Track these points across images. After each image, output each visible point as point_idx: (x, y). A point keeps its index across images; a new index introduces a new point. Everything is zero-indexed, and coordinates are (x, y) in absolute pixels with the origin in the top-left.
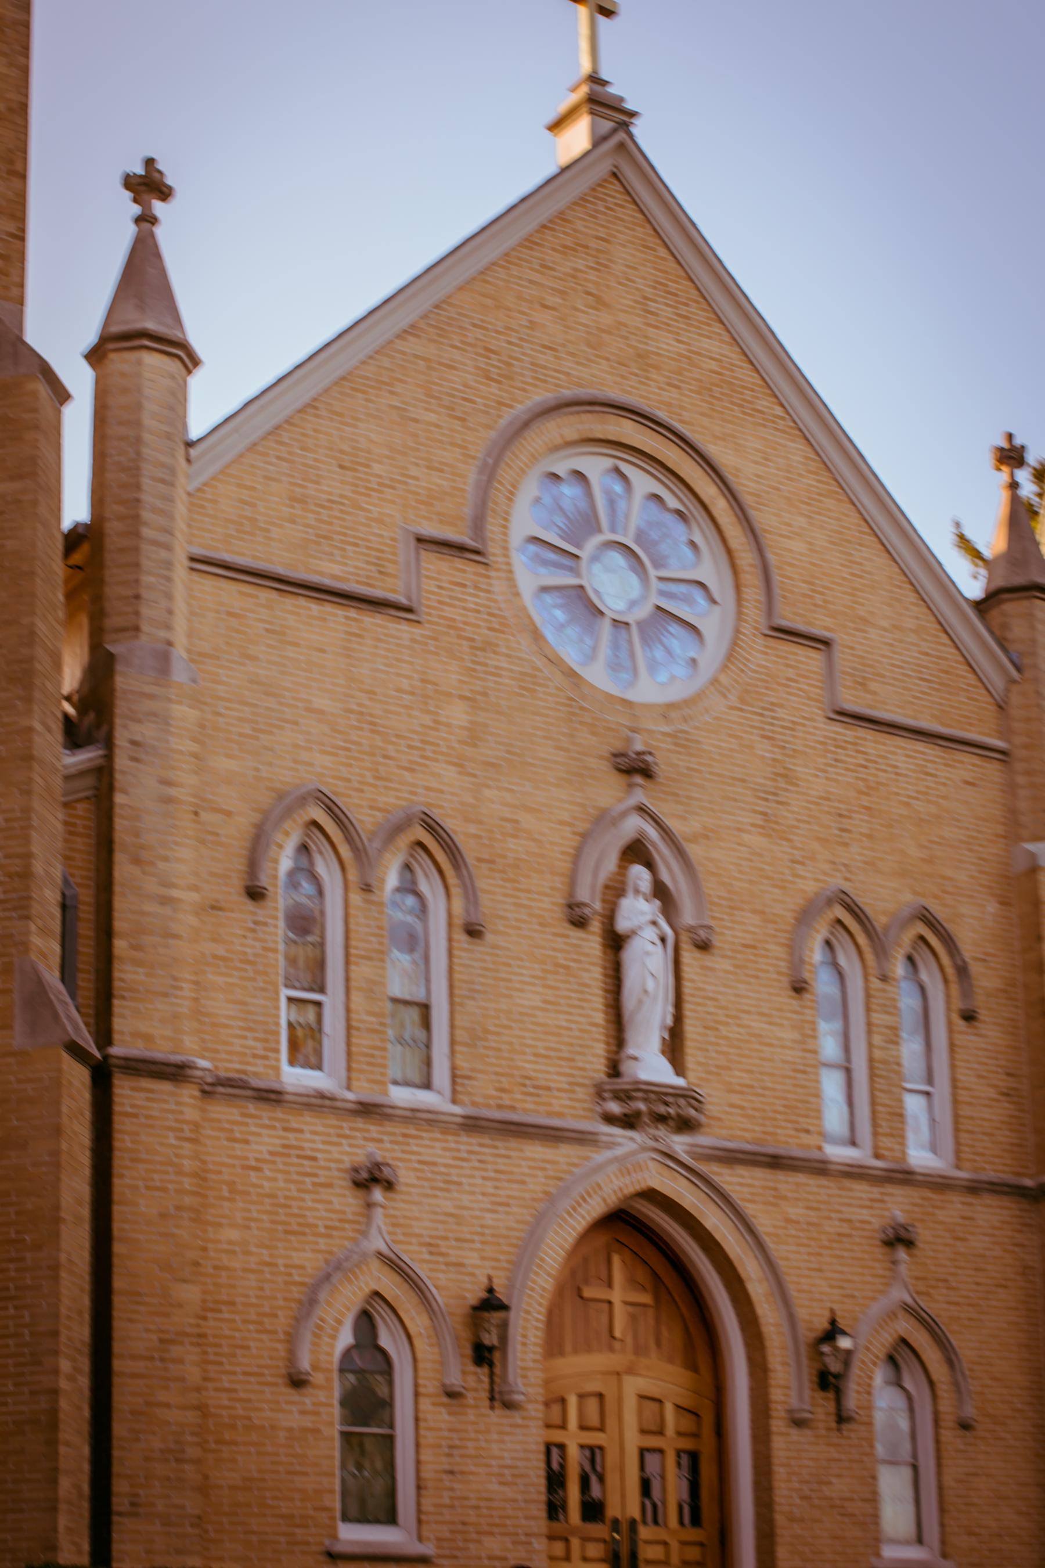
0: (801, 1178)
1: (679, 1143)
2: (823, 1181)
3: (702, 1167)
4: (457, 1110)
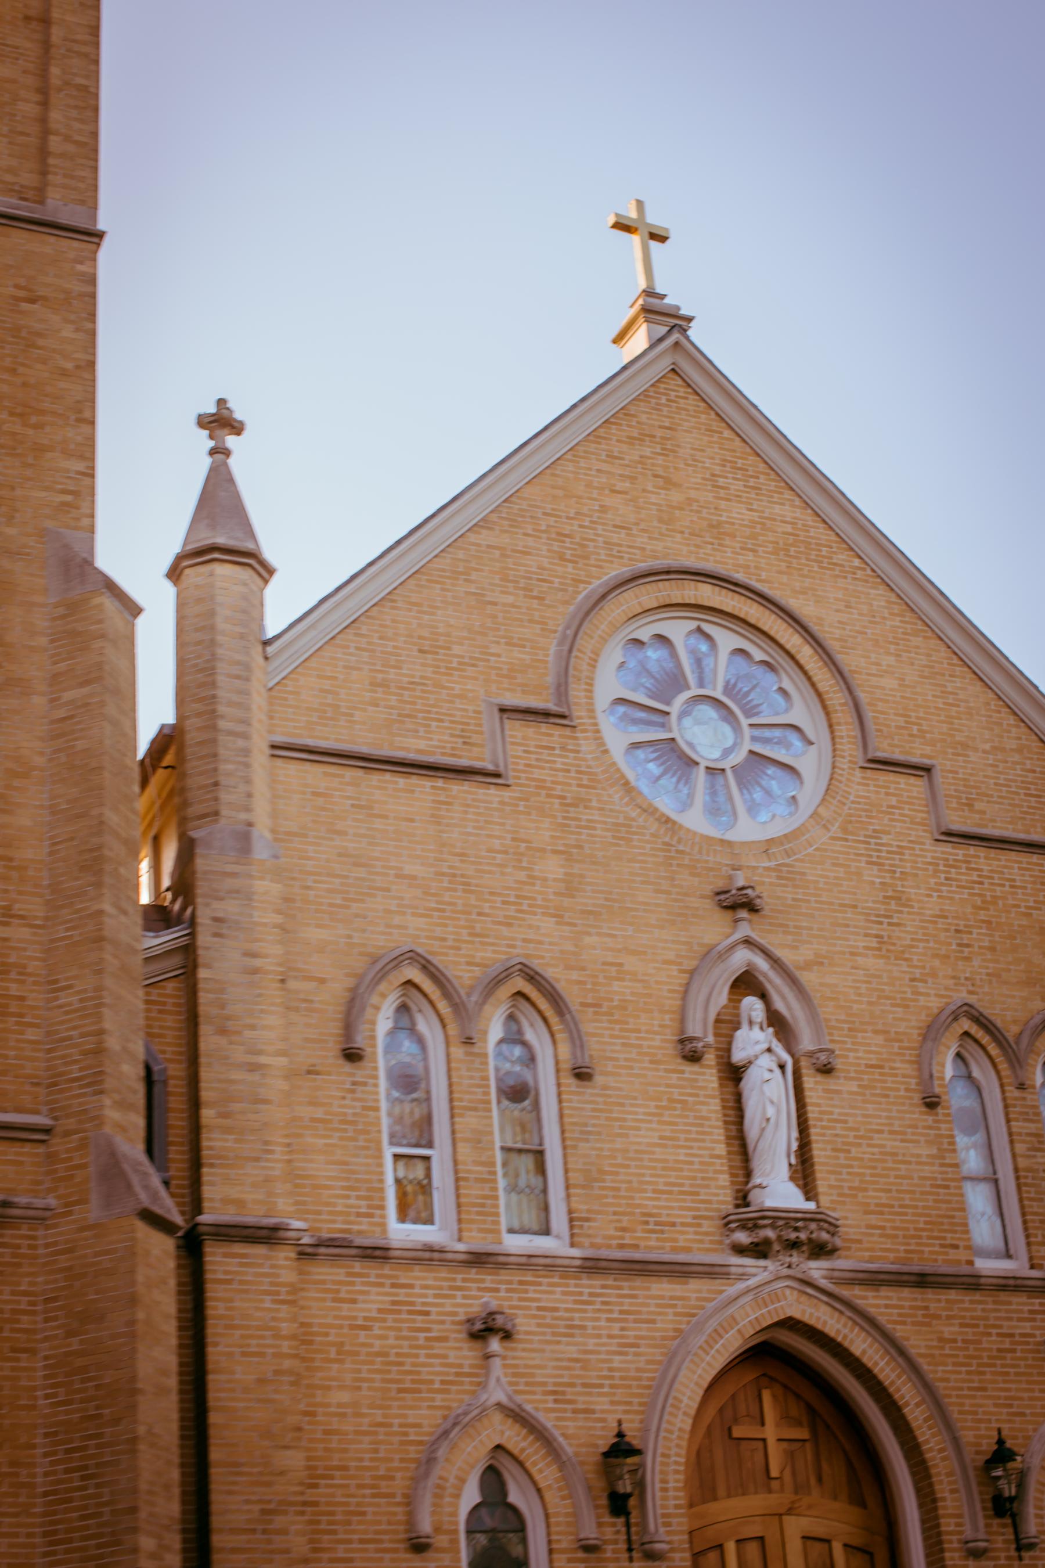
1: (817, 1269)
3: (845, 1292)
4: (576, 1252)
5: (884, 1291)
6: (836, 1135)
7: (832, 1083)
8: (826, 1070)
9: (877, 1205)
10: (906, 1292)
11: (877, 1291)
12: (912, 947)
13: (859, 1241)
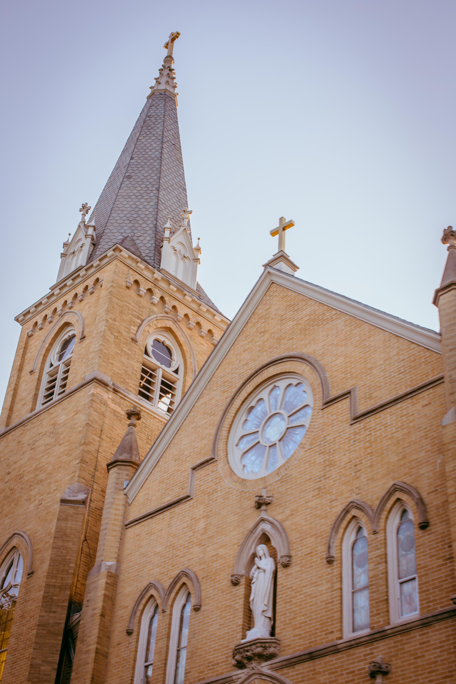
0: (328, 659)
2: (339, 655)
5: (298, 667)
6: (287, 596)
7: (289, 570)
8: (286, 566)
9: (300, 624)
10: (306, 664)
11: (294, 668)
12: (333, 485)
13: (289, 645)
